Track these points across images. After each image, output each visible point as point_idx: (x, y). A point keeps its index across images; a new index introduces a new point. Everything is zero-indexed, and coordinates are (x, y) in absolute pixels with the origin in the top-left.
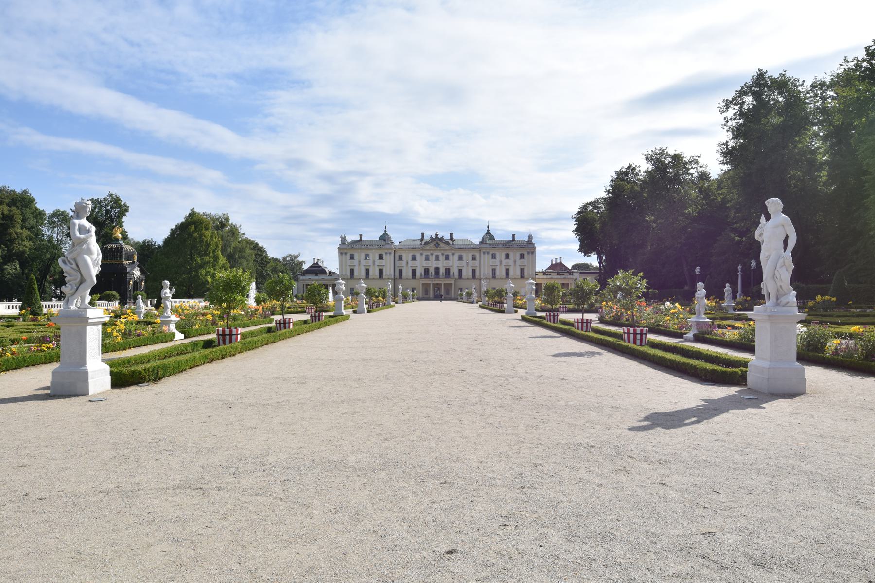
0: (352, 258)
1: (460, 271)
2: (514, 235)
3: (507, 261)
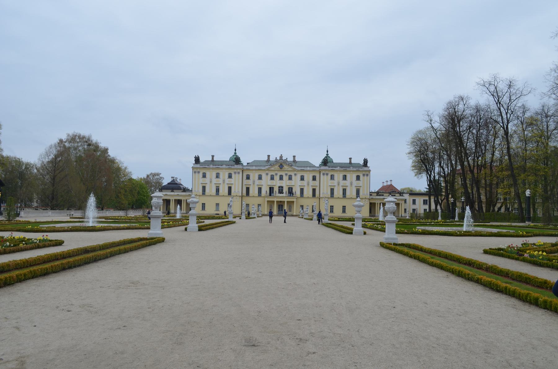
0: (204, 176)
1: (302, 190)
2: (350, 159)
3: (345, 182)
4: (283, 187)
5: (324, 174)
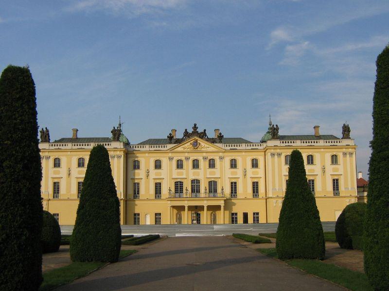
1: (234, 186)
4: (199, 181)
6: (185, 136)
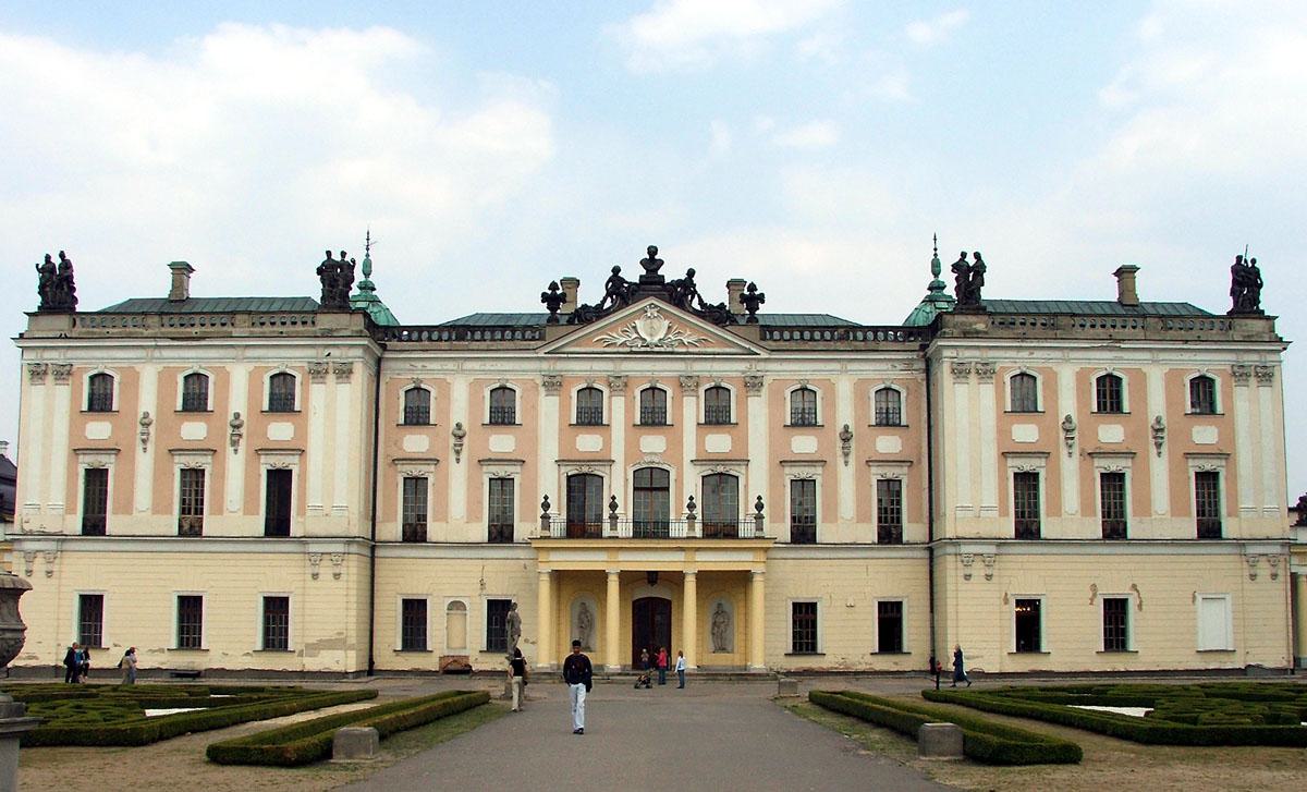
2: (1125, 274)
5: (960, 372)
6: (609, 294)
